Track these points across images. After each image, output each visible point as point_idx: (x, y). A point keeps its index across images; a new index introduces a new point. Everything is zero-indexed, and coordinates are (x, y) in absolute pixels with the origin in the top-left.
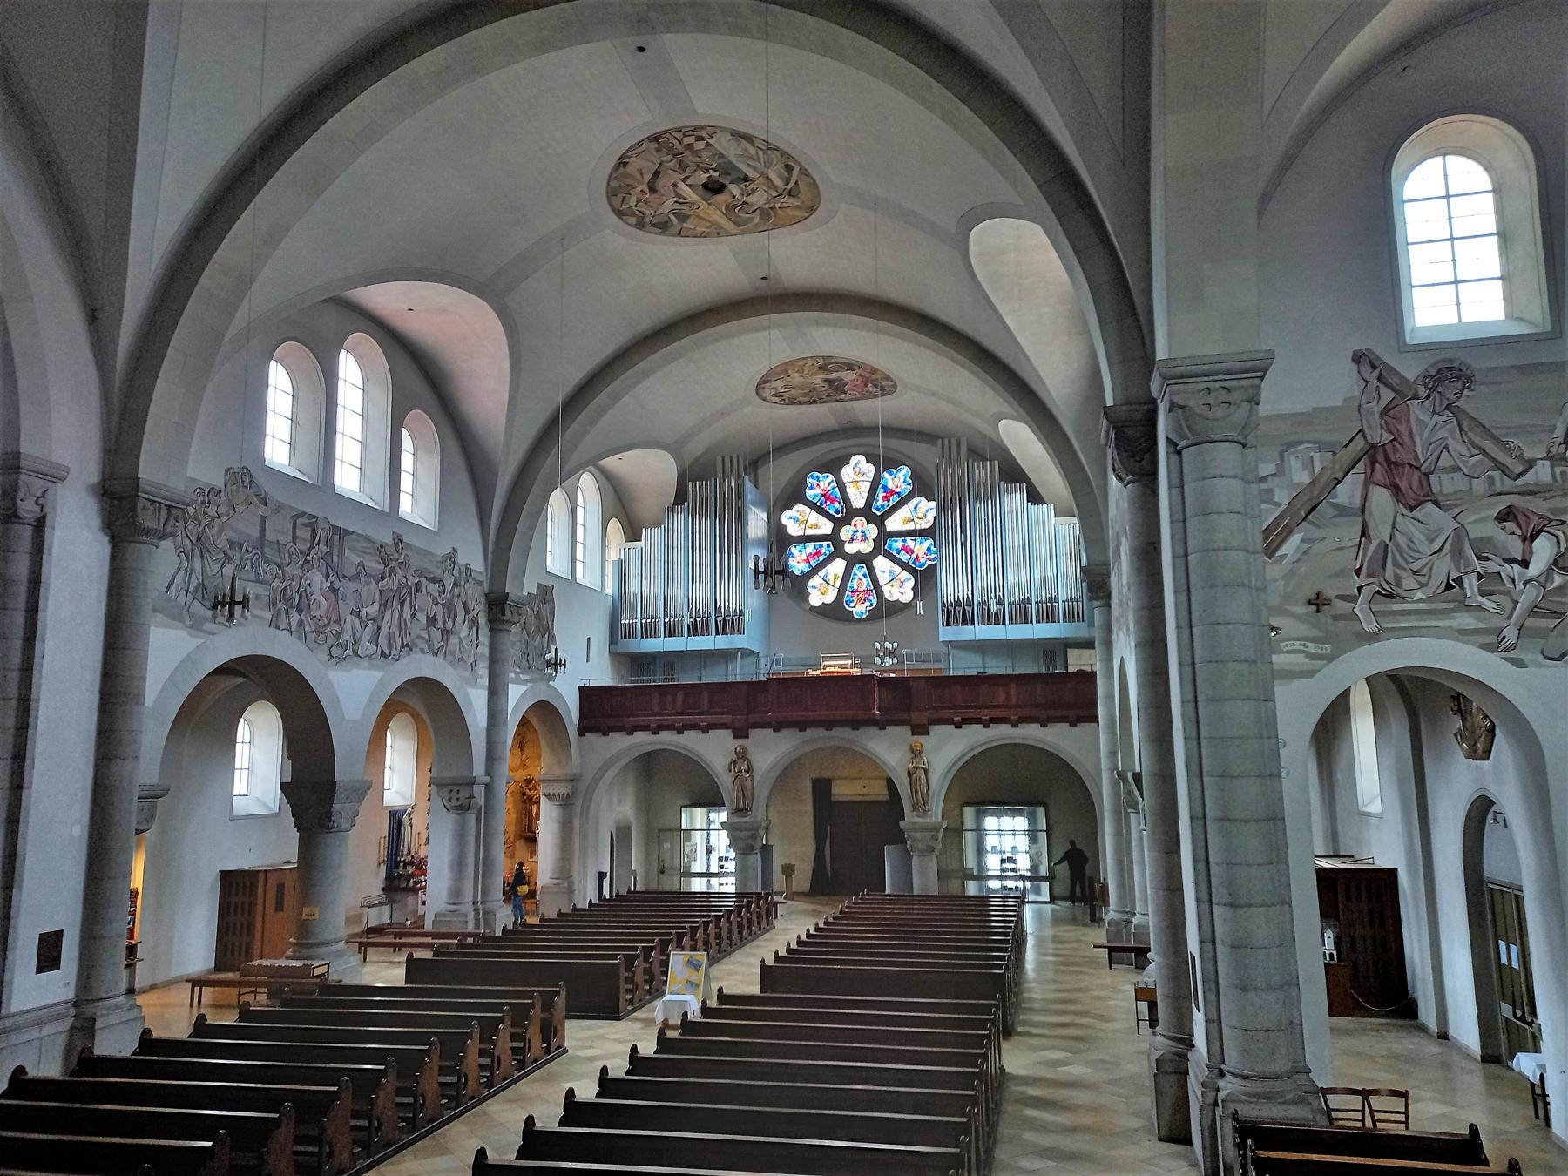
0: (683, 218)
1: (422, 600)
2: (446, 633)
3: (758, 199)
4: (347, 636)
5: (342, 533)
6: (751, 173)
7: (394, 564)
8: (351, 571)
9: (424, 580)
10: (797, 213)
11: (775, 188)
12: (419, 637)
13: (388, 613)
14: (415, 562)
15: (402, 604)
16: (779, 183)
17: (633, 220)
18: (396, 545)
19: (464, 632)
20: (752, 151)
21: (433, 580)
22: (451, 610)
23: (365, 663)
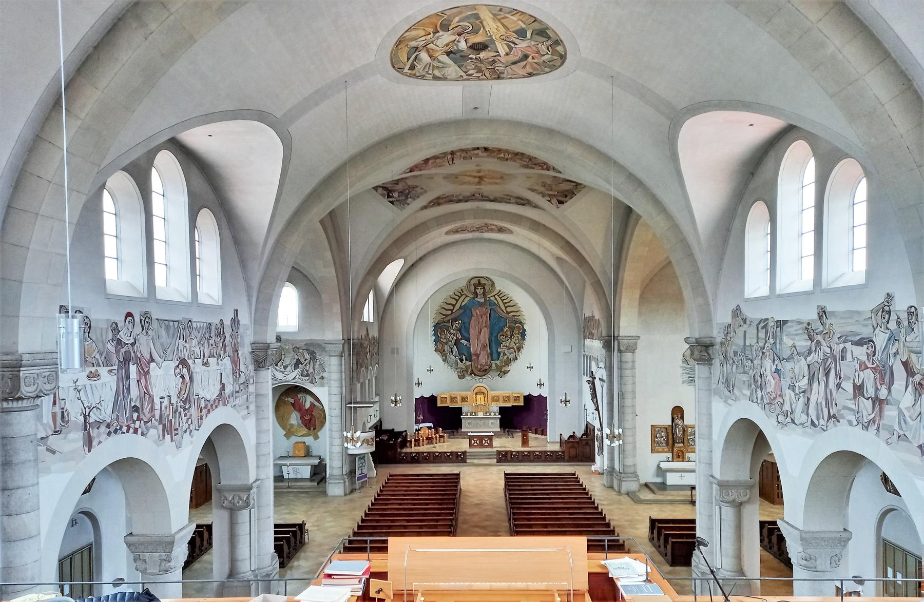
0: (521, 33)
1: (847, 368)
2: (878, 403)
3: (446, 38)
4: (787, 407)
5: (781, 324)
6: (445, 59)
7: (819, 338)
8: (786, 353)
9: (848, 345)
10: (413, 33)
11: (428, 51)
12: (845, 408)
13: (815, 385)
14: (838, 330)
15: (827, 374)
16: (424, 56)
17: (559, 49)
18: (820, 318)
19: (907, 399)
20: (437, 73)
21: (859, 343)
22: (885, 375)
23: (799, 429)
